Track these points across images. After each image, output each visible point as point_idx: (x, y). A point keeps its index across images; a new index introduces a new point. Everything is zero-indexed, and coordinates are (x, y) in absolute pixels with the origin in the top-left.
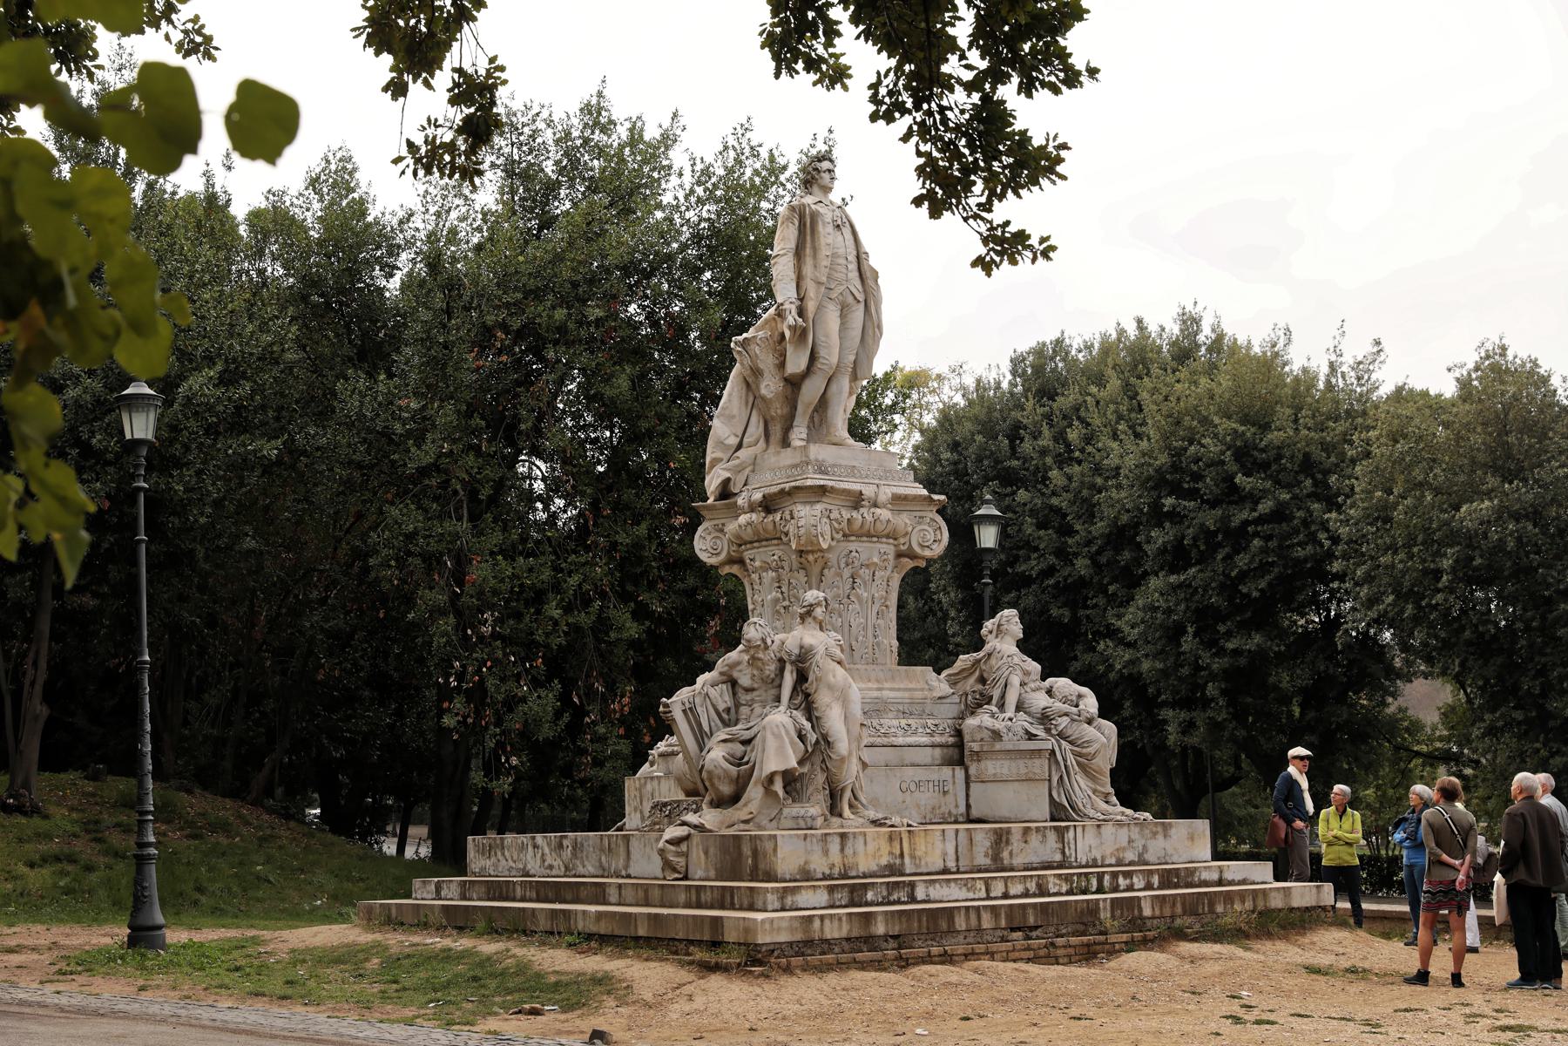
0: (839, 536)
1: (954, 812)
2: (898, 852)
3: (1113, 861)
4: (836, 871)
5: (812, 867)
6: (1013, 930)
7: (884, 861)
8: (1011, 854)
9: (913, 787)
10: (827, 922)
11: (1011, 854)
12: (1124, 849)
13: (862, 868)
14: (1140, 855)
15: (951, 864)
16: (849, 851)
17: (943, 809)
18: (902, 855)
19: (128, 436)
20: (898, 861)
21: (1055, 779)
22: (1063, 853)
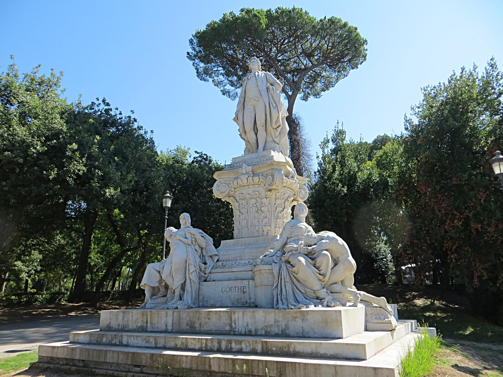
0: (233, 189)
1: (249, 301)
2: (145, 321)
3: (263, 333)
4: (120, 327)
5: (112, 325)
6: (135, 366)
7: (139, 325)
8: (200, 324)
9: (228, 290)
10: (59, 349)
11: (200, 324)
12: (271, 325)
13: (130, 327)
14: (282, 331)
15: (170, 328)
16: (125, 319)
17: (243, 300)
18: (147, 322)
19: (164, 205)
20: (145, 325)
21: (275, 285)
22: (231, 326)
